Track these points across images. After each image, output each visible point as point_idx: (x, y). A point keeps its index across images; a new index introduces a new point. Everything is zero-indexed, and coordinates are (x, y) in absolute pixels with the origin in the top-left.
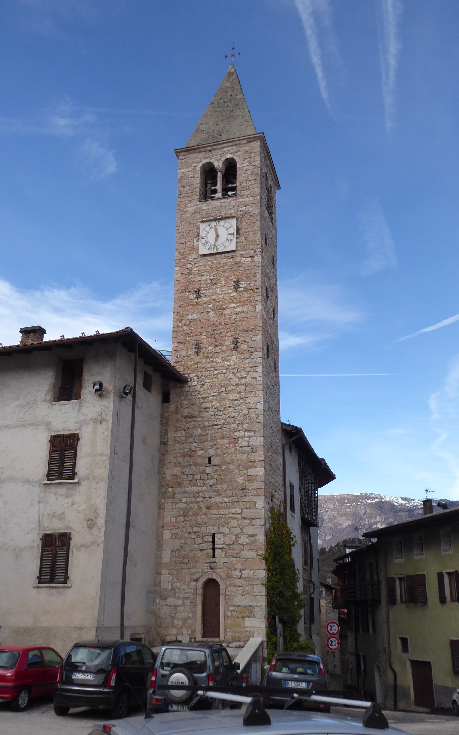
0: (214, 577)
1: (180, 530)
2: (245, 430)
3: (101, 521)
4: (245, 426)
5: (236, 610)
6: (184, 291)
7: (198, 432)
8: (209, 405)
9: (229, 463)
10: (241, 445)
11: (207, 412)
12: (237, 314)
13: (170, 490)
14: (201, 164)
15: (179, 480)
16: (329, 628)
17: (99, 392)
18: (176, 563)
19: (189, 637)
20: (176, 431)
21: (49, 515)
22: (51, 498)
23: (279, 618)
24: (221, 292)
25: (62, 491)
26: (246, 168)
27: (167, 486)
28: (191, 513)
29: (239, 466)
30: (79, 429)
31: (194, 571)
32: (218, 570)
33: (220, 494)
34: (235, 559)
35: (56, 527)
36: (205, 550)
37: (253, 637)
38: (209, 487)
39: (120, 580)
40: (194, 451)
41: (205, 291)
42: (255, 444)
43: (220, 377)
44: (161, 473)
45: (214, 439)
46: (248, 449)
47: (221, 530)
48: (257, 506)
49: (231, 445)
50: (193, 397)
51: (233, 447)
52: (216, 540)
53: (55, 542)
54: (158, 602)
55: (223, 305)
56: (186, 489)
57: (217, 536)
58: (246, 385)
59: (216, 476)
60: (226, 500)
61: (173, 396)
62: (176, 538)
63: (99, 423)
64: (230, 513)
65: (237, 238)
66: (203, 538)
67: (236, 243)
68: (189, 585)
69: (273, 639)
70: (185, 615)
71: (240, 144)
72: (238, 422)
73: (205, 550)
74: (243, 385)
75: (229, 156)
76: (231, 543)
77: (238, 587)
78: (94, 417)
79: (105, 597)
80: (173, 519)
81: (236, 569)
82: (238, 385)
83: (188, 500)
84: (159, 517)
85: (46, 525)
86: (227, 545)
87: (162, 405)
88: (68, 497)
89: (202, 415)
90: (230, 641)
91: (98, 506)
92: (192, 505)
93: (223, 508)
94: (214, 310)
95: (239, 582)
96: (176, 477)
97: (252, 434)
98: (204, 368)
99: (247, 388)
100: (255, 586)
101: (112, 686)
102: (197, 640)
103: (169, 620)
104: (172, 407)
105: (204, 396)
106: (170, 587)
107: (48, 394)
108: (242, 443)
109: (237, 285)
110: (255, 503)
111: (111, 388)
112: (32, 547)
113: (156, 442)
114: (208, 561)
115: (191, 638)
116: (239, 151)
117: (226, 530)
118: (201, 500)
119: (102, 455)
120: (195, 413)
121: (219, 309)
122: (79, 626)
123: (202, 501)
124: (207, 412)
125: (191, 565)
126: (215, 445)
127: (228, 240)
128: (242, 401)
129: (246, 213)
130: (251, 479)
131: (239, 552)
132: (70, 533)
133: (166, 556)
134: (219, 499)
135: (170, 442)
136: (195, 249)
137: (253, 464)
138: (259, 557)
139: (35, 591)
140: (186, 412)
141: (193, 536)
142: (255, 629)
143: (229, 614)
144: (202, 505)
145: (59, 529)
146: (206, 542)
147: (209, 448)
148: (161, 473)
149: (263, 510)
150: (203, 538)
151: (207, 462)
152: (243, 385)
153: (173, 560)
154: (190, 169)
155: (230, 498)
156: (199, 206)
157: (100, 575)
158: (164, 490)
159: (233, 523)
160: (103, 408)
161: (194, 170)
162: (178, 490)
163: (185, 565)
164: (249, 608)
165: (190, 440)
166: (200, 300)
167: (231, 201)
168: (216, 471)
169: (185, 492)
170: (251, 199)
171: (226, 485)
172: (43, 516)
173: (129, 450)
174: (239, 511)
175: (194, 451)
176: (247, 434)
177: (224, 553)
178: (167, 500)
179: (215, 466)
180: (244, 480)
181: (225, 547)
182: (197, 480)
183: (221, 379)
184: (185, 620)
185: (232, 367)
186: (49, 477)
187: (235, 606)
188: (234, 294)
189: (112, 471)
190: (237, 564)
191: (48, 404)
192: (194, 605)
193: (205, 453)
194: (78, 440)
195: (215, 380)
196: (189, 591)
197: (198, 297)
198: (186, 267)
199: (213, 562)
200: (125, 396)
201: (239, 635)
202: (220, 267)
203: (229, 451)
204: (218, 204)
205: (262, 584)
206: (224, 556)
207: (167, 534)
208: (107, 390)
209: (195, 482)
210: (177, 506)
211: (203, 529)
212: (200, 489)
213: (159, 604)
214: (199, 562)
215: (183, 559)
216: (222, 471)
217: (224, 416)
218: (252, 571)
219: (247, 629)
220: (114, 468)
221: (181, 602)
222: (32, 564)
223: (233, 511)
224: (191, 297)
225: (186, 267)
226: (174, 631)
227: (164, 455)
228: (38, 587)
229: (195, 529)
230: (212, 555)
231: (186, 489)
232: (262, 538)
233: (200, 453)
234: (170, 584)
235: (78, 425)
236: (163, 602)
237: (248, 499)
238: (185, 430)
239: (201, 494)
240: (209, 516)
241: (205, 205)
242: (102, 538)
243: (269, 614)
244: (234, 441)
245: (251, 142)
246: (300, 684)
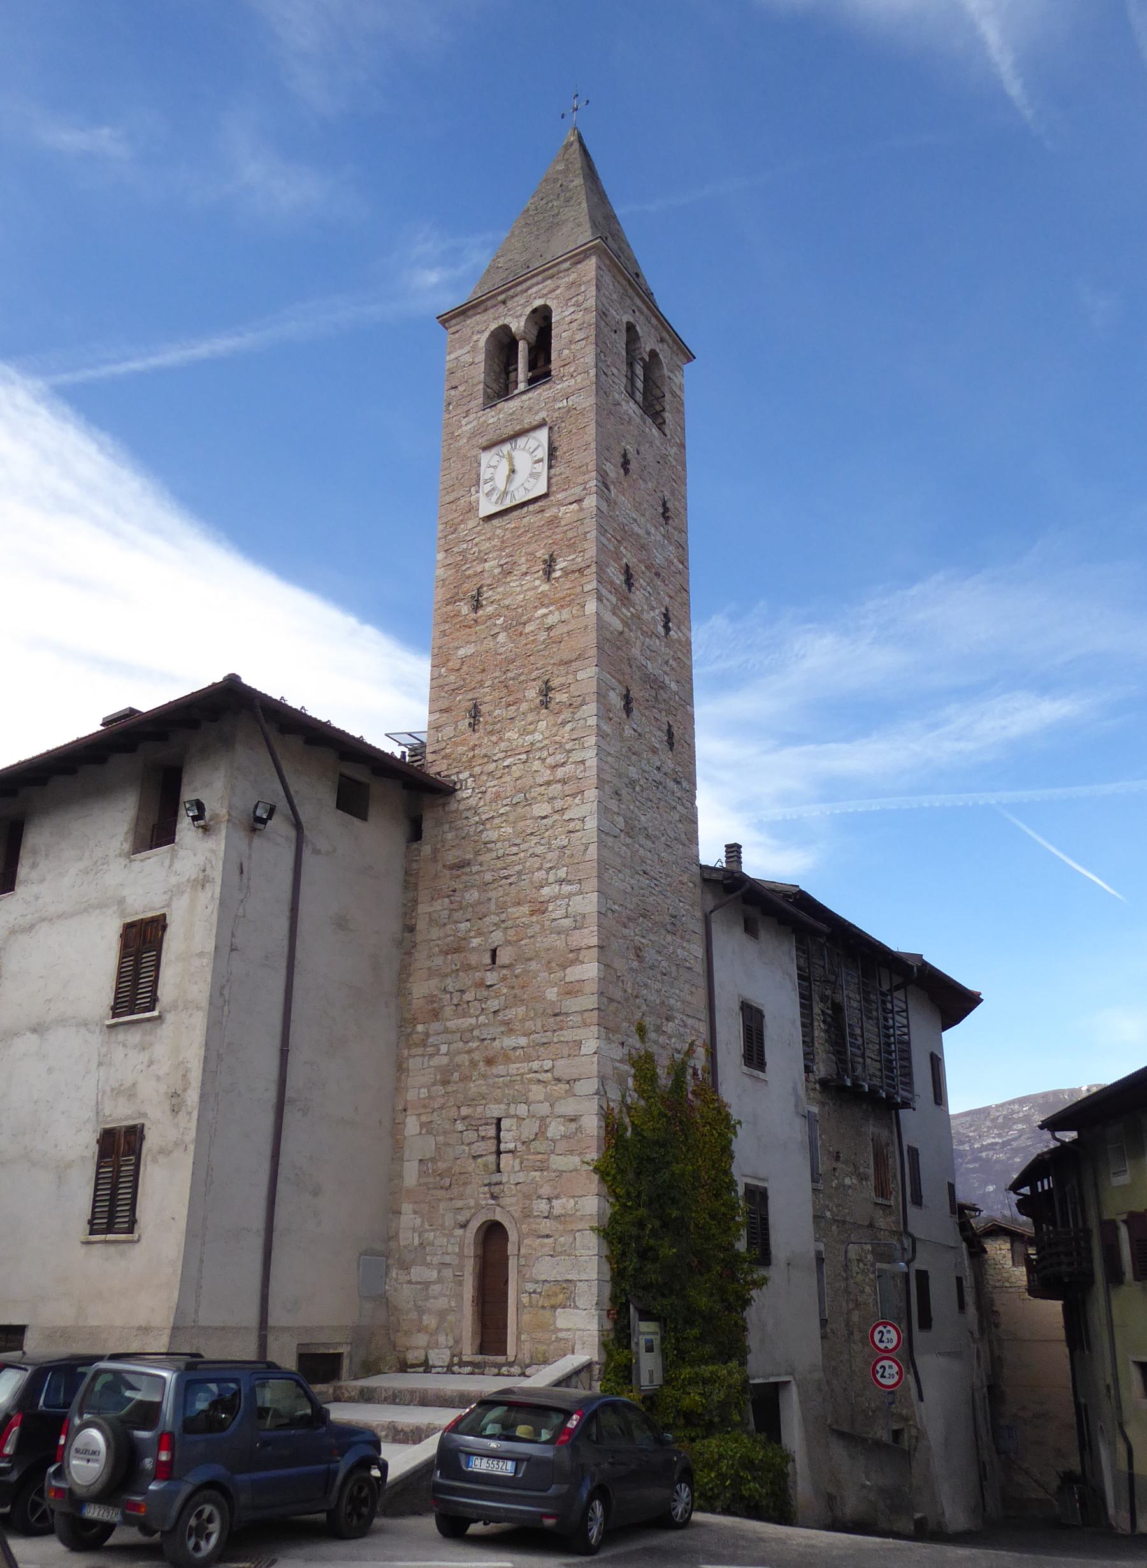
0: (498, 1218)
1: (435, 1114)
2: (561, 882)
3: (192, 1097)
4: (562, 873)
5: (539, 1290)
6: (452, 601)
7: (473, 895)
8: (492, 835)
9: (530, 959)
10: (554, 916)
11: (490, 850)
12: (549, 629)
13: (420, 1028)
14: (487, 334)
15: (435, 1005)
17: (202, 822)
18: (428, 1189)
19: (448, 1352)
20: (433, 899)
21: (112, 1090)
22: (119, 1053)
23: (636, 1308)
24: (518, 589)
25: (134, 1037)
26: (568, 319)
27: (414, 1021)
28: (456, 1075)
29: (549, 962)
30: (168, 905)
31: (459, 1204)
32: (506, 1201)
33: (511, 1030)
34: (538, 1174)
35: (120, 1115)
36: (481, 1156)
37: (573, 1353)
38: (491, 1015)
39: (257, 1221)
40: (464, 939)
41: (490, 593)
42: (581, 909)
43: (516, 771)
44: (401, 992)
45: (502, 908)
46: (567, 922)
47: (512, 1112)
48: (584, 1051)
49: (534, 918)
50: (465, 822)
51: (537, 922)
52: (502, 1134)
53: (119, 1148)
54: (394, 1275)
55: (522, 615)
56: (448, 1024)
57: (505, 1124)
58: (564, 782)
59: (505, 991)
60: (523, 1041)
61: (427, 826)
62: (429, 1132)
63: (200, 888)
64: (532, 1071)
65: (550, 467)
66: (477, 1130)
67: (549, 479)
68: (452, 1235)
69: (621, 1358)
70: (442, 1303)
71: (559, 272)
72: (548, 865)
73: (481, 1156)
74: (559, 781)
75: (538, 303)
76: (532, 1137)
77: (543, 1237)
78: (193, 878)
79: (202, 1261)
80: (424, 1092)
81: (539, 1197)
82: (548, 783)
83: (453, 1046)
84: (398, 1089)
85: (107, 1113)
86: (524, 1143)
87: (407, 847)
88: (144, 1049)
89: (480, 858)
90: (527, 1361)
91: (189, 1065)
92: (458, 1059)
93: (518, 1060)
94: (505, 629)
95: (546, 1226)
96: (431, 999)
97: (574, 888)
98: (485, 756)
99: (566, 787)
100: (577, 1234)
101: (7, 1456)
102: (465, 1358)
103: (414, 1315)
104: (426, 849)
105: (484, 817)
106: (416, 1242)
107: (126, 840)
108: (556, 911)
110: (579, 1044)
111: (223, 812)
112: (83, 1159)
114: (486, 1182)
115: (453, 1356)
116: (558, 287)
117: (522, 1110)
118: (475, 1045)
119: (201, 954)
120: (467, 857)
121: (515, 626)
122: (143, 1324)
123: (477, 1048)
124: (490, 850)
125: (455, 1191)
126: (503, 921)
127: (532, 475)
128: (556, 817)
129: (569, 411)
130: (572, 990)
131: (546, 1156)
132: (143, 1125)
133: (411, 1174)
134: (509, 1042)
135: (421, 925)
136: (472, 508)
137: (574, 956)
138: (586, 1167)
139: (83, 1250)
140: (451, 857)
141: (460, 1126)
142: (578, 1333)
143: (525, 1299)
144: (476, 1056)
145: (126, 1119)
146: (483, 1137)
147: (492, 929)
149: (595, 1059)
150: (477, 1130)
151: (489, 961)
152: (559, 781)
153: (422, 1181)
154: (467, 348)
155: (532, 1037)
156: (482, 420)
157: (185, 1212)
158: (409, 1030)
159: (537, 1092)
160: (208, 855)
161: (474, 349)
162: (435, 1026)
163: (443, 1192)
164: (564, 1285)
165: (457, 916)
166: (480, 612)
167: (540, 394)
168: (504, 979)
169: (446, 1031)
170: (579, 379)
171: (524, 1008)
172: (104, 1092)
173: (286, 943)
174: (548, 1064)
175: (464, 939)
176: (566, 888)
177: (517, 1161)
178: (413, 1051)
179: (503, 967)
180: (559, 994)
181: (520, 1147)
182: (468, 1002)
183: (518, 774)
184: (442, 1314)
185: (539, 745)
186: (116, 1011)
187: (537, 1282)
188: (545, 587)
189: (223, 987)
190: (542, 1187)
191: (123, 861)
192: (459, 1281)
193: (486, 941)
194: (164, 927)
195: (507, 778)
196: (450, 1249)
197: (477, 606)
198: (456, 550)
199: (496, 1184)
200: (260, 826)
201: (545, 1347)
202: (519, 536)
203: (530, 932)
205: (592, 1229)
206: (517, 1168)
207: (412, 1125)
208: (214, 817)
209: (465, 1006)
210: (431, 1063)
211: (479, 1109)
212: (473, 1021)
213: (396, 1280)
214: (471, 1183)
215: (443, 1180)
216: (516, 977)
217: (522, 854)
218: (572, 1201)
219: (561, 1335)
220: (228, 980)
221: (435, 1273)
223: (535, 1065)
224: (465, 609)
225: (456, 550)
226: (421, 1340)
227: (409, 954)
228: (88, 1243)
229: (465, 1111)
230: (494, 1167)
231: (448, 1024)
232: (592, 1124)
233: (475, 942)
234: (416, 1235)
235: (166, 897)
236: (403, 1277)
237: (568, 1035)
238: (449, 896)
239: (476, 1033)
240: (491, 1081)
241: (493, 413)
242: (192, 1134)
243: (614, 1298)
244: (539, 909)
245: (579, 262)
246: (501, 1464)
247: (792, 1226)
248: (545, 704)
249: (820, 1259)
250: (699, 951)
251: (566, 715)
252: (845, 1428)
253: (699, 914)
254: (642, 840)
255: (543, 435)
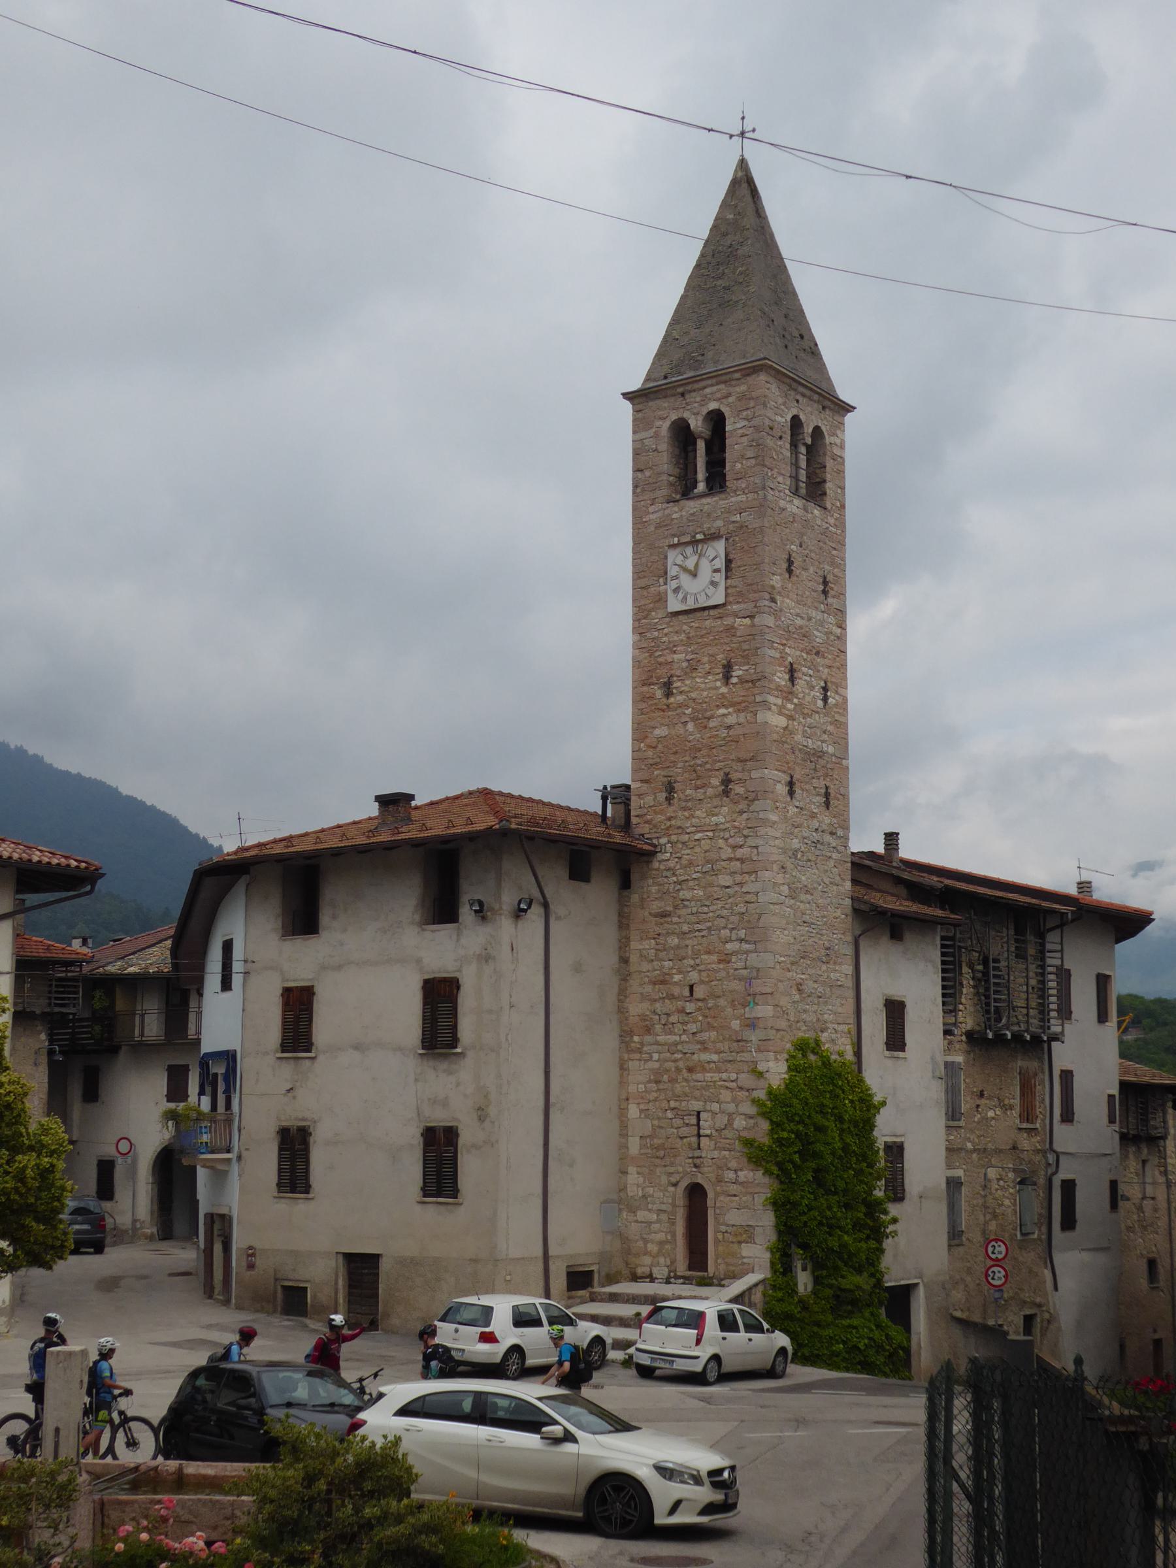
0: (700, 1181)
2: (741, 940)
4: (742, 934)
11: (686, 907)
12: (729, 727)
13: (636, 1039)
14: (667, 424)
16: (990, 1249)
24: (703, 686)
26: (740, 431)
27: (631, 1033)
28: (666, 1077)
30: (459, 971)
31: (672, 1169)
34: (727, 1153)
35: (440, 1118)
41: (679, 684)
43: (705, 844)
45: (696, 955)
49: (721, 966)
52: (701, 1123)
55: (706, 710)
57: (703, 1116)
58: (742, 860)
60: (715, 1057)
61: (634, 877)
62: (647, 1117)
64: (721, 1080)
65: (727, 578)
67: (726, 588)
70: (661, 1236)
71: (731, 380)
74: (738, 860)
75: (713, 406)
80: (642, 1087)
81: (729, 1169)
82: (730, 859)
83: (662, 1055)
94: (694, 719)
95: (733, 1188)
96: (643, 1017)
98: (679, 827)
99: (744, 866)
103: (640, 1244)
104: (635, 898)
105: (682, 878)
106: (640, 1194)
108: (737, 962)
109: (728, 669)
113: (613, 959)
115: (670, 1272)
116: (729, 395)
118: (678, 1056)
121: (702, 720)
125: (667, 1160)
127: (714, 584)
128: (737, 888)
129: (742, 527)
134: (705, 1057)
135: (634, 958)
136: (661, 599)
139: (418, 1208)
140: (655, 906)
141: (670, 1114)
144: (681, 1064)
146: (687, 1125)
148: (621, 1011)
151: (688, 994)
152: (738, 860)
154: (651, 432)
156: (667, 512)
159: (726, 1095)
161: (656, 435)
162: (648, 1038)
165: (663, 954)
166: (672, 700)
167: (717, 502)
168: (699, 1009)
169: (657, 1043)
170: (751, 496)
173: (543, 993)
176: (746, 946)
178: (631, 1056)
179: (698, 1000)
183: (707, 847)
185: (722, 827)
187: (728, 1226)
188: (724, 690)
192: (672, 1222)
195: (697, 849)
197: (668, 694)
198: (649, 635)
202: (702, 637)
204: (703, 507)
206: (712, 1147)
207: (633, 1111)
211: (684, 1104)
219: (745, 1260)
221: (655, 1216)
222: (413, 1169)
223: (724, 1076)
224: (659, 693)
225: (649, 635)
226: (647, 1260)
227: (625, 980)
229: (673, 1104)
233: (677, 978)
236: (631, 1218)
237: (746, 1056)
239: (680, 1047)
240: (692, 1084)
241: (676, 509)
244: (725, 959)
245: (748, 375)
247: (925, 1168)
248: (726, 793)
249: (953, 1185)
250: (848, 969)
251: (743, 805)
252: (976, 1318)
253: (849, 938)
254: (803, 897)
255: (720, 547)
